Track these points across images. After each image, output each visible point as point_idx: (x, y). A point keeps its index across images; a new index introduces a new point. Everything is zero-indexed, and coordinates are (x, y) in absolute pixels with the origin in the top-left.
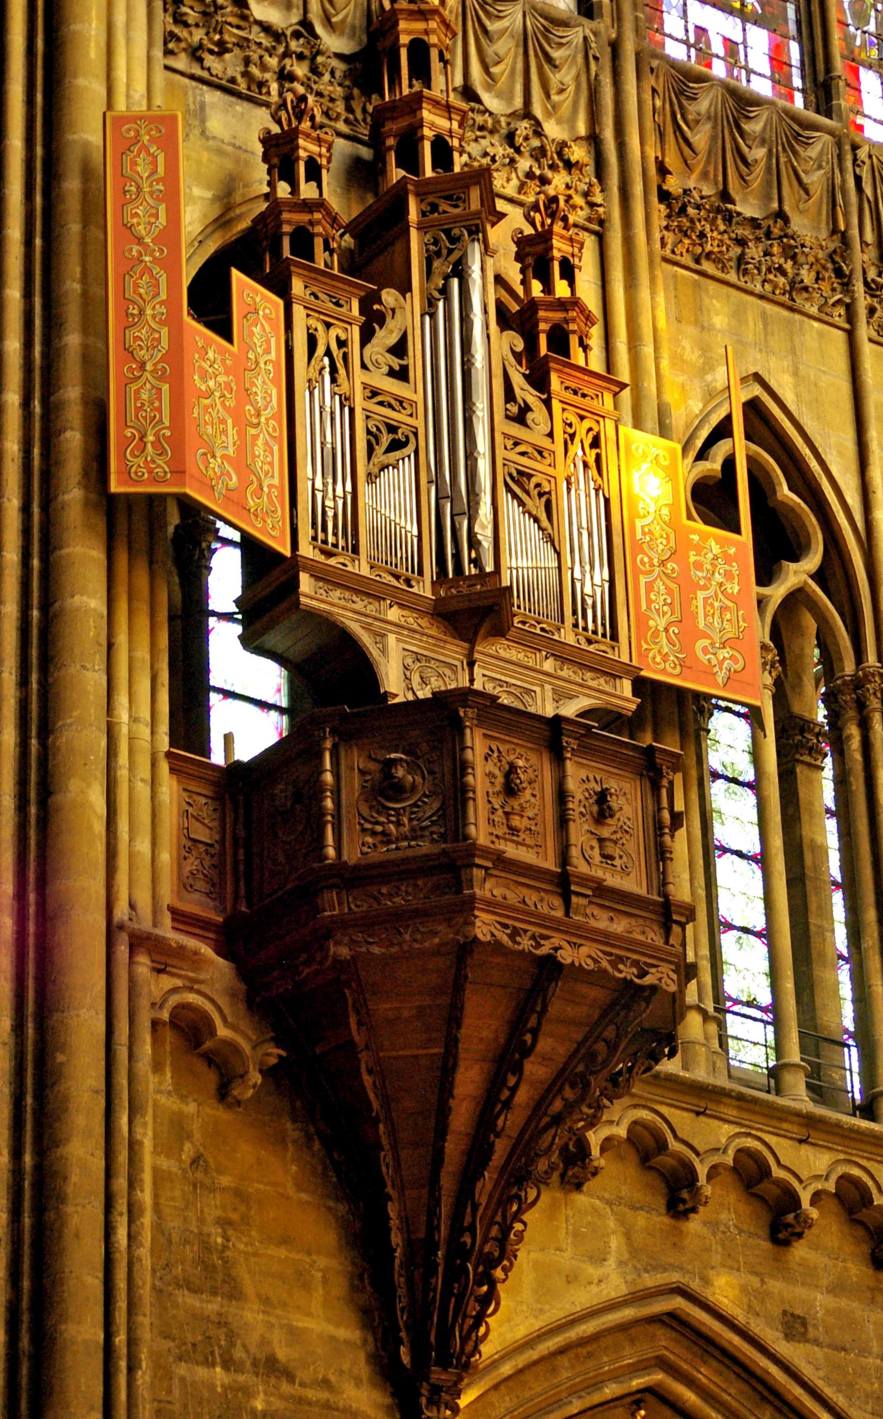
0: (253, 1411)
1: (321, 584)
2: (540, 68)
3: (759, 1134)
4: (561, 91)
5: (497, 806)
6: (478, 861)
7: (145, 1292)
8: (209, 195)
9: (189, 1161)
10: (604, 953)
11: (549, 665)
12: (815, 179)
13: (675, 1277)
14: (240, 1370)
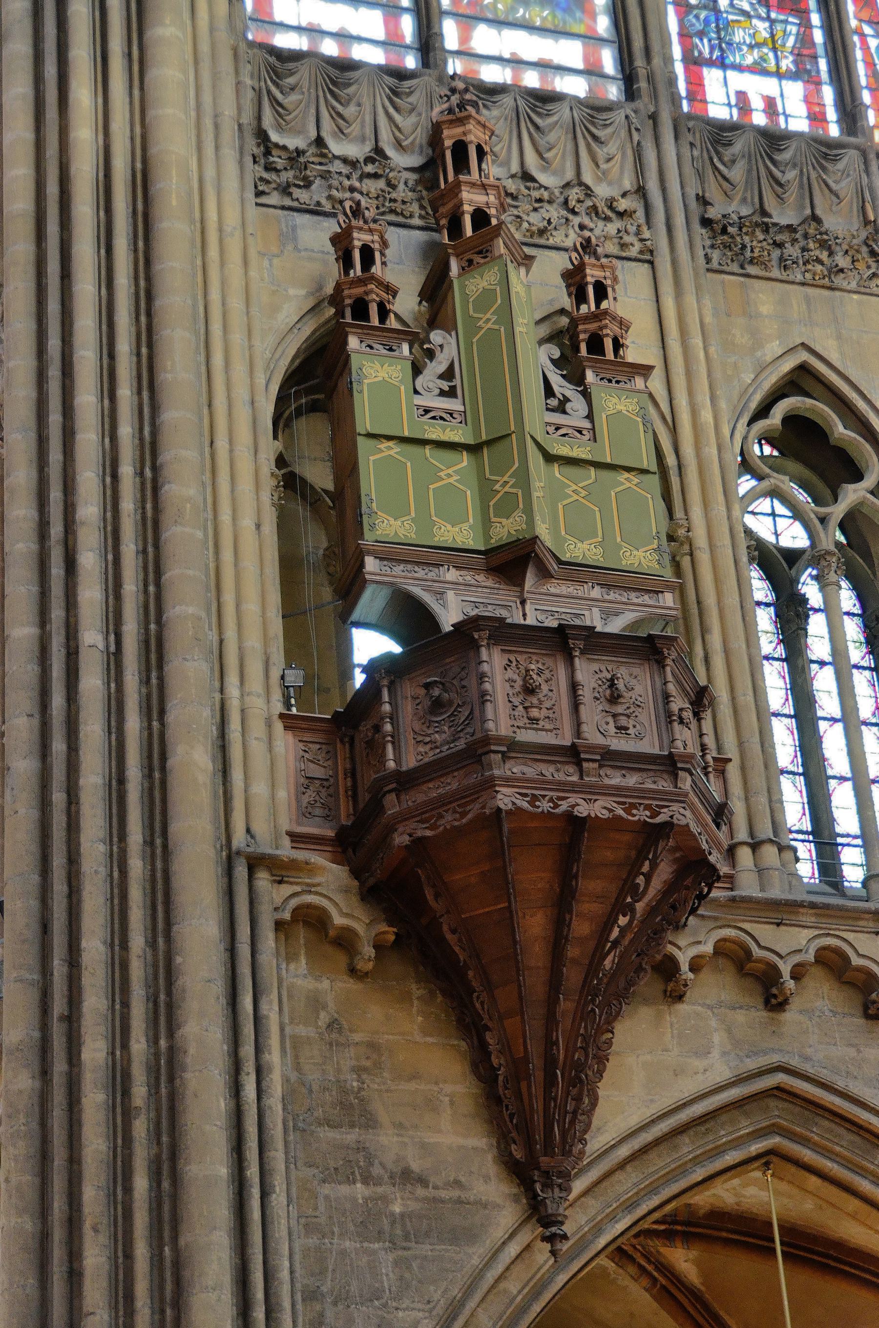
0: (392, 1214)
1: (385, 563)
2: (588, 146)
3: (837, 933)
4: (609, 160)
5: (517, 704)
6: (493, 748)
7: (276, 1131)
8: (303, 292)
9: (325, 1026)
10: (618, 803)
11: (596, 592)
12: (845, 187)
13: (775, 1059)
14: (378, 1182)
